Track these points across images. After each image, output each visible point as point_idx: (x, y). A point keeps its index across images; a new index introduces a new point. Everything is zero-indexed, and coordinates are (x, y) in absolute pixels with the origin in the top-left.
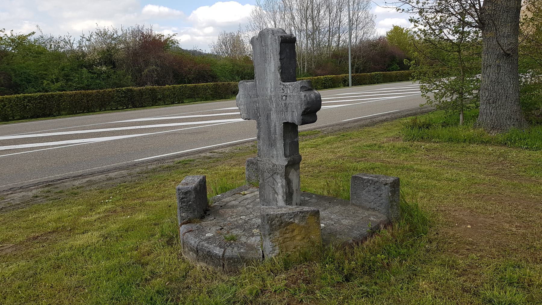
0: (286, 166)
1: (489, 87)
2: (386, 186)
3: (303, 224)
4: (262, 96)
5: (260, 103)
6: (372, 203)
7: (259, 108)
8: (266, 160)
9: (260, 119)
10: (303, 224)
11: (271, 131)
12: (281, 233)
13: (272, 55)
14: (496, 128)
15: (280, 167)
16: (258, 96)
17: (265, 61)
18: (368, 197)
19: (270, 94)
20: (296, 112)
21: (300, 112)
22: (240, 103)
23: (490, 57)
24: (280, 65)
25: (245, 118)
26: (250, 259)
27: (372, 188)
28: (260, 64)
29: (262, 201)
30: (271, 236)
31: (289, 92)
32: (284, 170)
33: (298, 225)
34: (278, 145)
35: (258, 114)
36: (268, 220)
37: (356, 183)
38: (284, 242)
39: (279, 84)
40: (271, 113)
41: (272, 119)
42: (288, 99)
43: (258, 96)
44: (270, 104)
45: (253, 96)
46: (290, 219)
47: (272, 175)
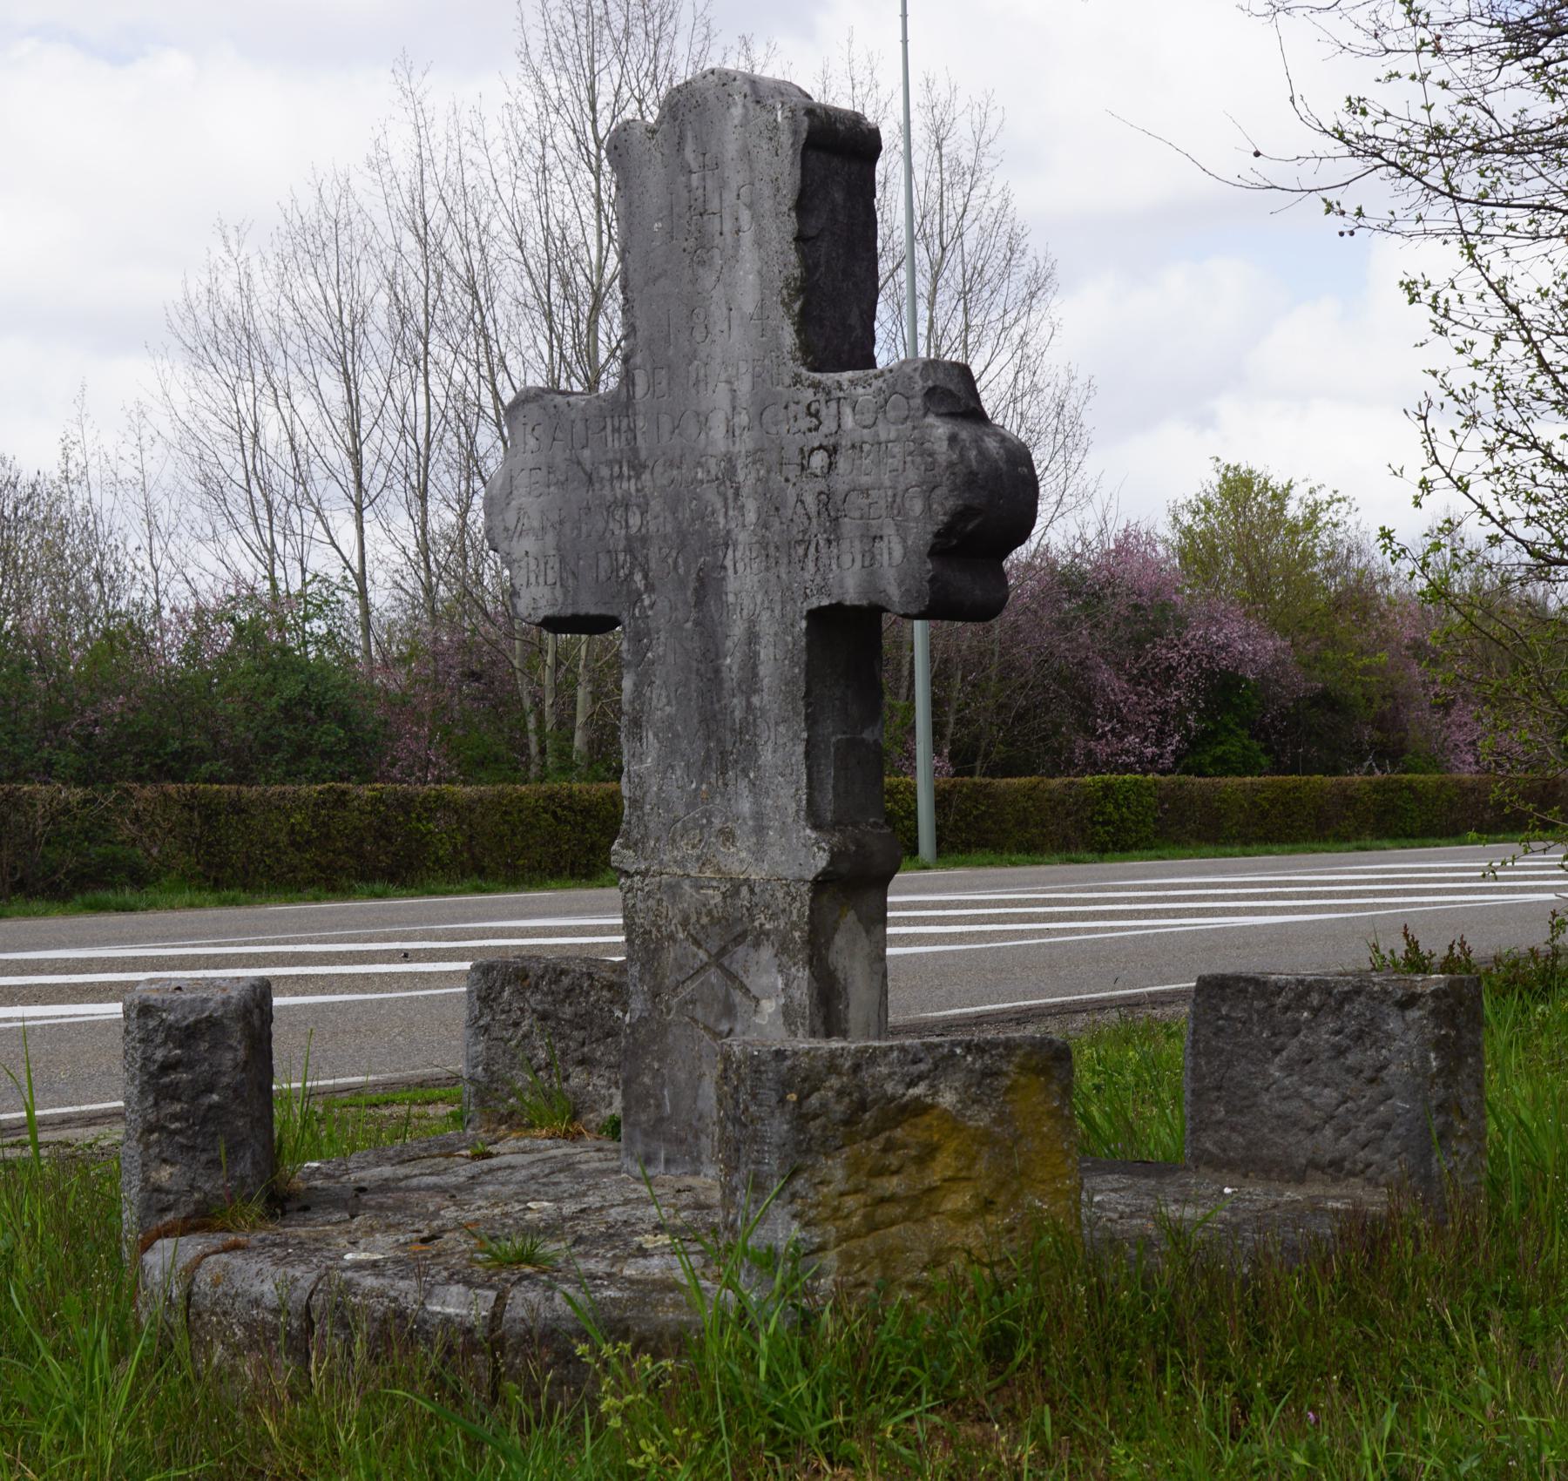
0: (820, 884)
2: (1413, 1014)
3: (982, 1118)
4: (671, 465)
5: (656, 505)
6: (1328, 1132)
7: (645, 540)
8: (681, 863)
9: (652, 606)
10: (982, 1118)
11: (725, 674)
12: (854, 1167)
13: (745, 216)
15: (780, 895)
16: (638, 468)
17: (700, 249)
18: (1298, 1094)
20: (895, 540)
21: (921, 533)
22: (511, 523)
24: (797, 273)
26: (661, 1335)
27: (1324, 1036)
28: (664, 274)
30: (799, 1184)
31: (849, 421)
32: (801, 908)
33: (953, 1122)
34: (767, 756)
35: (638, 577)
36: (785, 1085)
37: (1227, 1018)
38: (872, 1226)
39: (788, 381)
40: (729, 563)
41: (731, 598)
42: (842, 463)
43: (638, 468)
44: (719, 505)
45: (605, 472)
46: (912, 1084)
47: (723, 951)
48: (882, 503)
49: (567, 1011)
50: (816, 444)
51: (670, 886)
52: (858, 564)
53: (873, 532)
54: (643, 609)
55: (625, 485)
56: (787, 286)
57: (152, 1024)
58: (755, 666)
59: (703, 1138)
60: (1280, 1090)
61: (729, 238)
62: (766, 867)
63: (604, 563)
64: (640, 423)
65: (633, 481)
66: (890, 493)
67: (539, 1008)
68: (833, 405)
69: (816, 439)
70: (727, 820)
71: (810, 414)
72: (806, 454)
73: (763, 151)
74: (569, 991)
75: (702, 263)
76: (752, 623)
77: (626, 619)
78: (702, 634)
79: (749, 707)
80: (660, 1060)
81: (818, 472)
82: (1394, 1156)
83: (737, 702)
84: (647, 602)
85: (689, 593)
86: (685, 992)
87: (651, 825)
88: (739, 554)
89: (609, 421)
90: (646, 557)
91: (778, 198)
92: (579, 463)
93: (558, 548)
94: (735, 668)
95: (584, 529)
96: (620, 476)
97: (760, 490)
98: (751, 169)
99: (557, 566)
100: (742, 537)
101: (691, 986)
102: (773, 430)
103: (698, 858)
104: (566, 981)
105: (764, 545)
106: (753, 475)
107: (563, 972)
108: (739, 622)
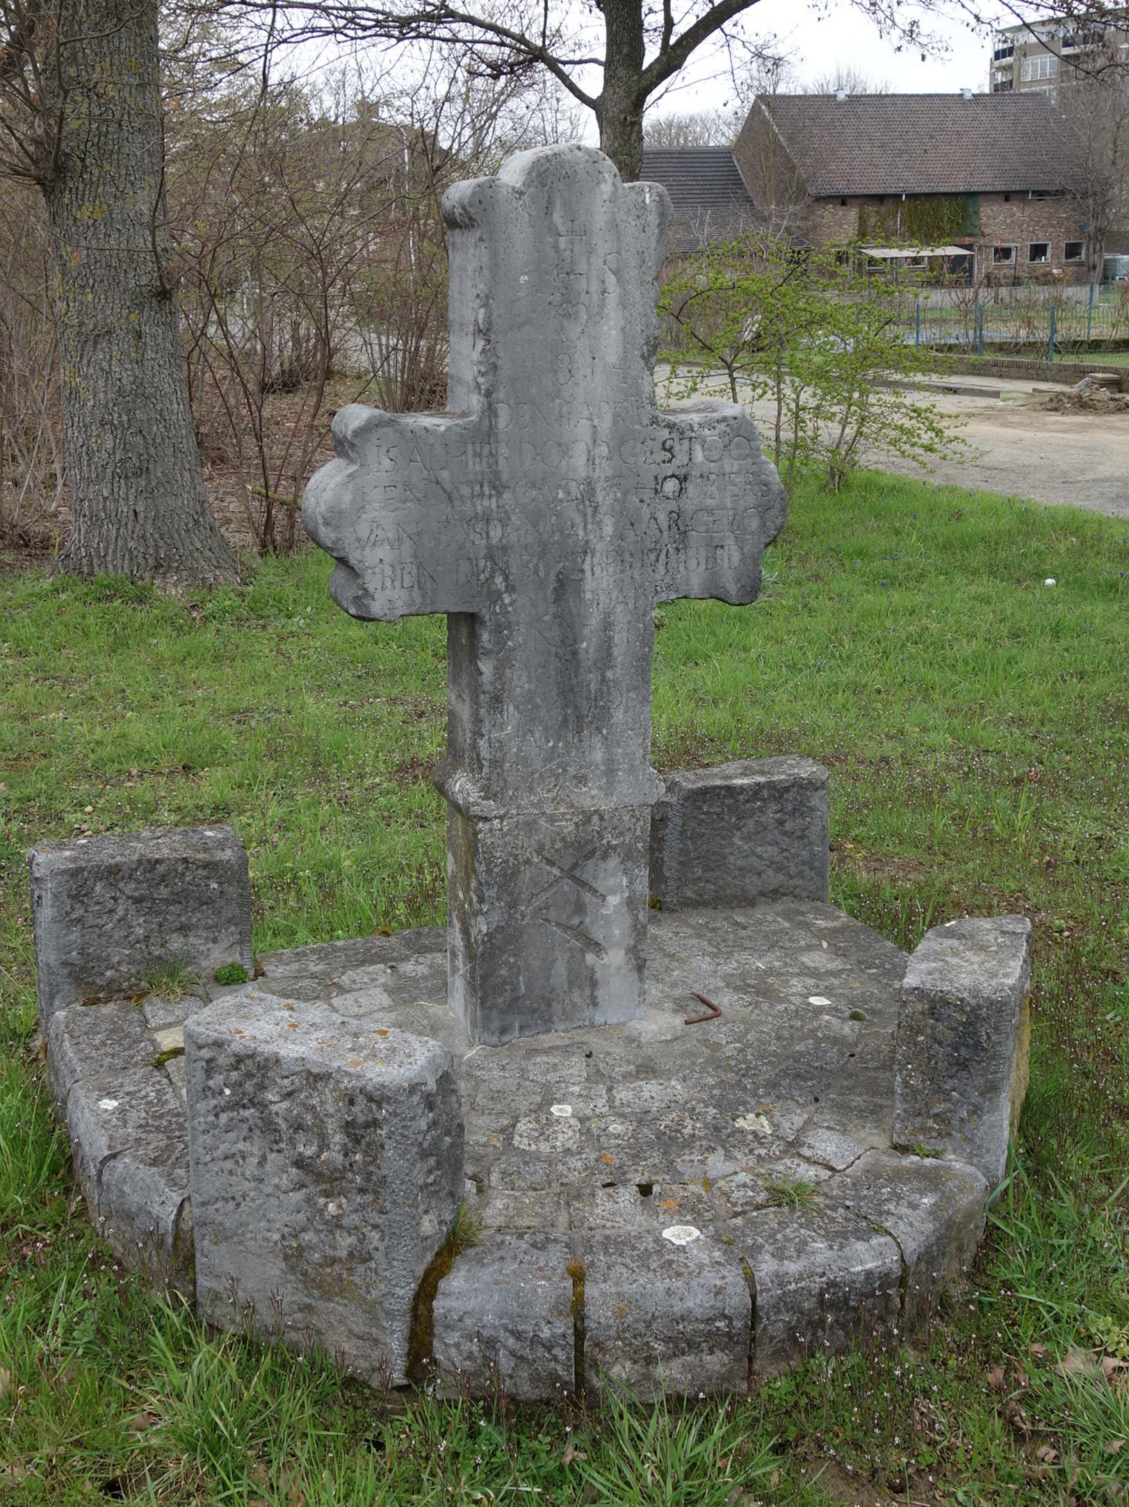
1: (116, 416)
4: (533, 485)
7: (505, 549)
9: (511, 604)
11: (582, 656)
13: (611, 280)
14: (170, 567)
15: (626, 818)
16: (498, 488)
17: (568, 303)
18: (754, 853)
19: (582, 472)
20: (734, 548)
23: (106, 298)
25: (399, 612)
27: (771, 814)
29: (494, 1014)
31: (699, 456)
34: (618, 716)
35: (499, 580)
39: (646, 421)
40: (587, 567)
41: (588, 595)
42: (691, 488)
43: (498, 488)
44: (578, 520)
45: (465, 491)
48: (725, 520)
49: (164, 892)
50: (670, 473)
51: (527, 824)
52: (703, 566)
53: (716, 542)
54: (503, 606)
55: (486, 502)
56: (647, 344)
57: (416, 1099)
58: (609, 648)
59: (555, 1004)
60: (740, 853)
61: (595, 298)
62: (615, 799)
63: (465, 567)
64: (503, 451)
65: (494, 499)
66: (731, 513)
67: (136, 894)
68: (686, 443)
69: (669, 469)
70: (581, 768)
71: (664, 449)
72: (659, 481)
73: (630, 228)
74: (163, 878)
75: (568, 316)
76: (607, 615)
77: (485, 614)
78: (560, 625)
79: (604, 680)
80: (515, 955)
81: (670, 495)
82: (812, 879)
83: (593, 679)
84: (507, 601)
85: (549, 592)
86: (537, 903)
87: (510, 779)
88: (596, 560)
89: (470, 447)
90: (507, 563)
91: (643, 269)
92: (438, 483)
93: (415, 555)
94: (591, 650)
95: (444, 539)
96: (482, 495)
97: (617, 508)
98: (619, 241)
99: (414, 572)
100: (600, 546)
101: (543, 897)
102: (632, 460)
103: (554, 799)
104: (161, 869)
105: (619, 552)
106: (611, 496)
107: (157, 861)
108: (596, 614)
